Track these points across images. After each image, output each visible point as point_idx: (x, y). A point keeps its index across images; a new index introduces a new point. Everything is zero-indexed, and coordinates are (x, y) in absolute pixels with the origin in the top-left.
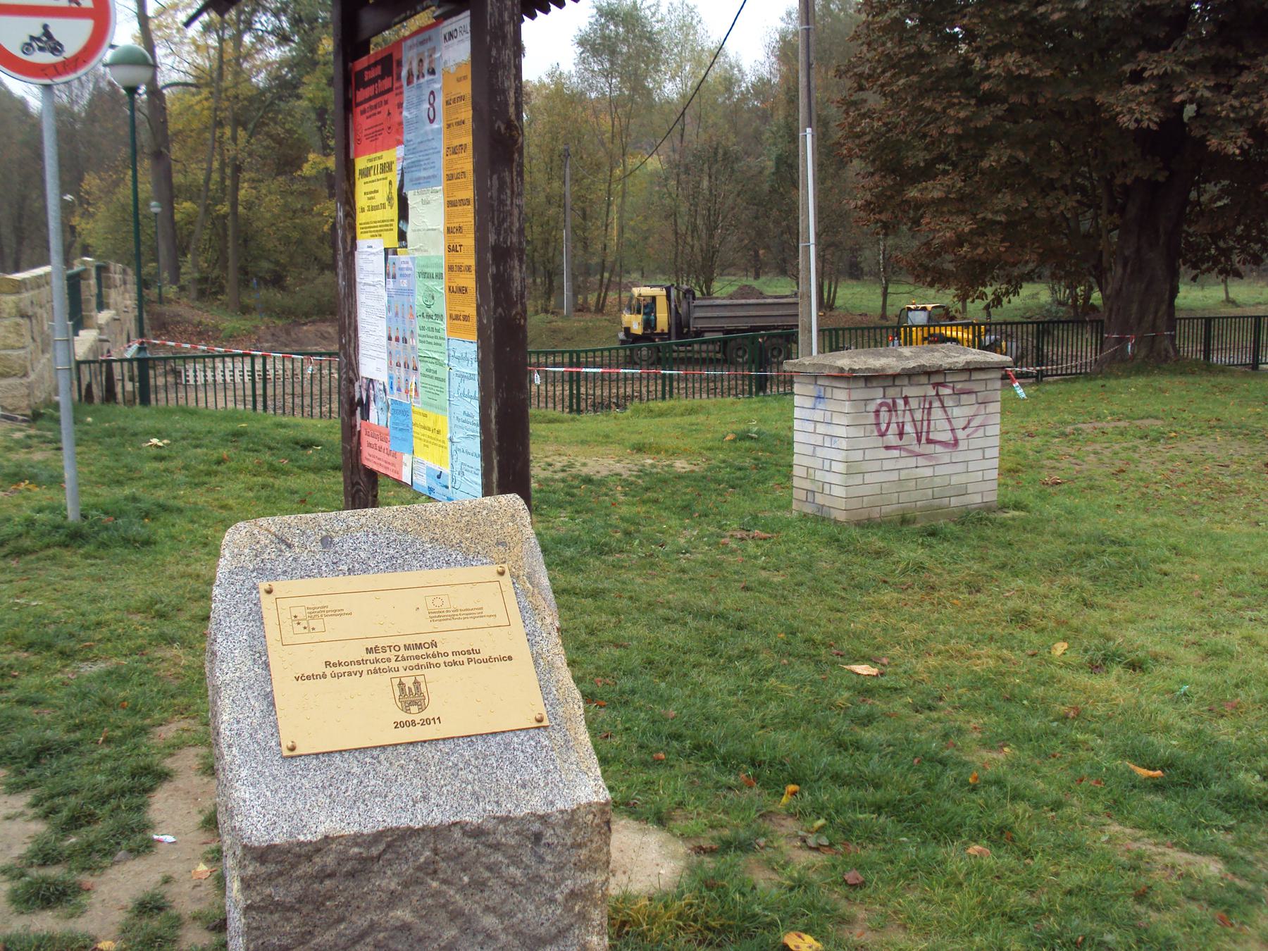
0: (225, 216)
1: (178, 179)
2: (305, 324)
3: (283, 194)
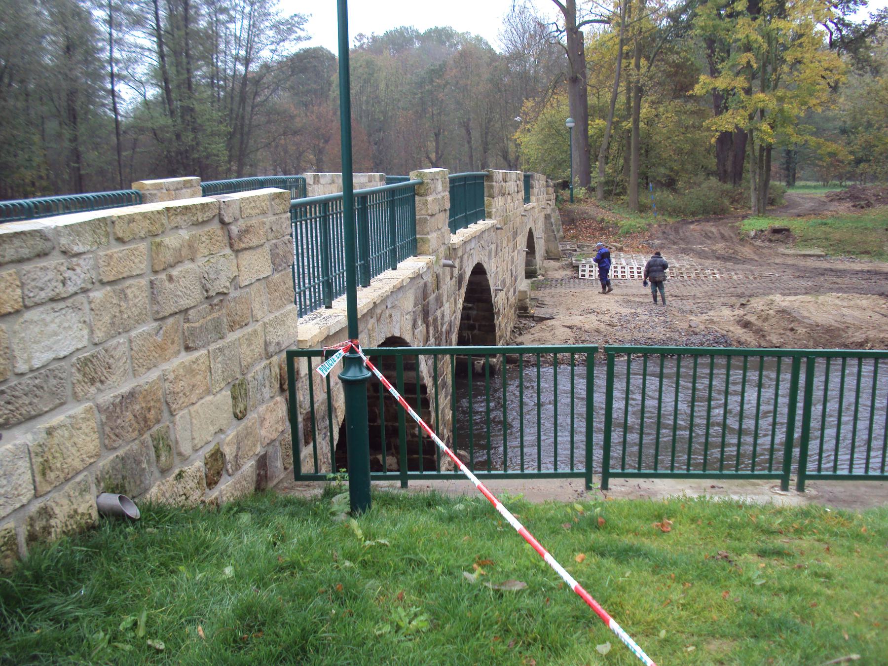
0: (629, 131)
1: (592, 100)
2: (692, 223)
3: (677, 113)
